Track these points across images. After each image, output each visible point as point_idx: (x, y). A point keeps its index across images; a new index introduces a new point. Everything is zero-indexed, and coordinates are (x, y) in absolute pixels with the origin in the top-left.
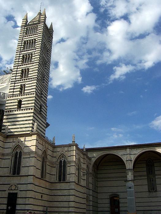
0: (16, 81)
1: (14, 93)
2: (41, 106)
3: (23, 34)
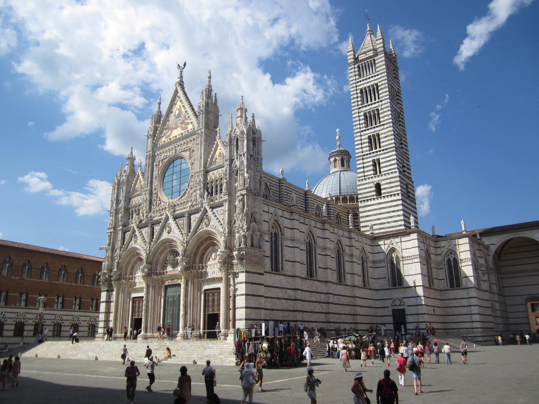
0: (364, 155)
1: (366, 174)
2: (407, 186)
3: (354, 78)
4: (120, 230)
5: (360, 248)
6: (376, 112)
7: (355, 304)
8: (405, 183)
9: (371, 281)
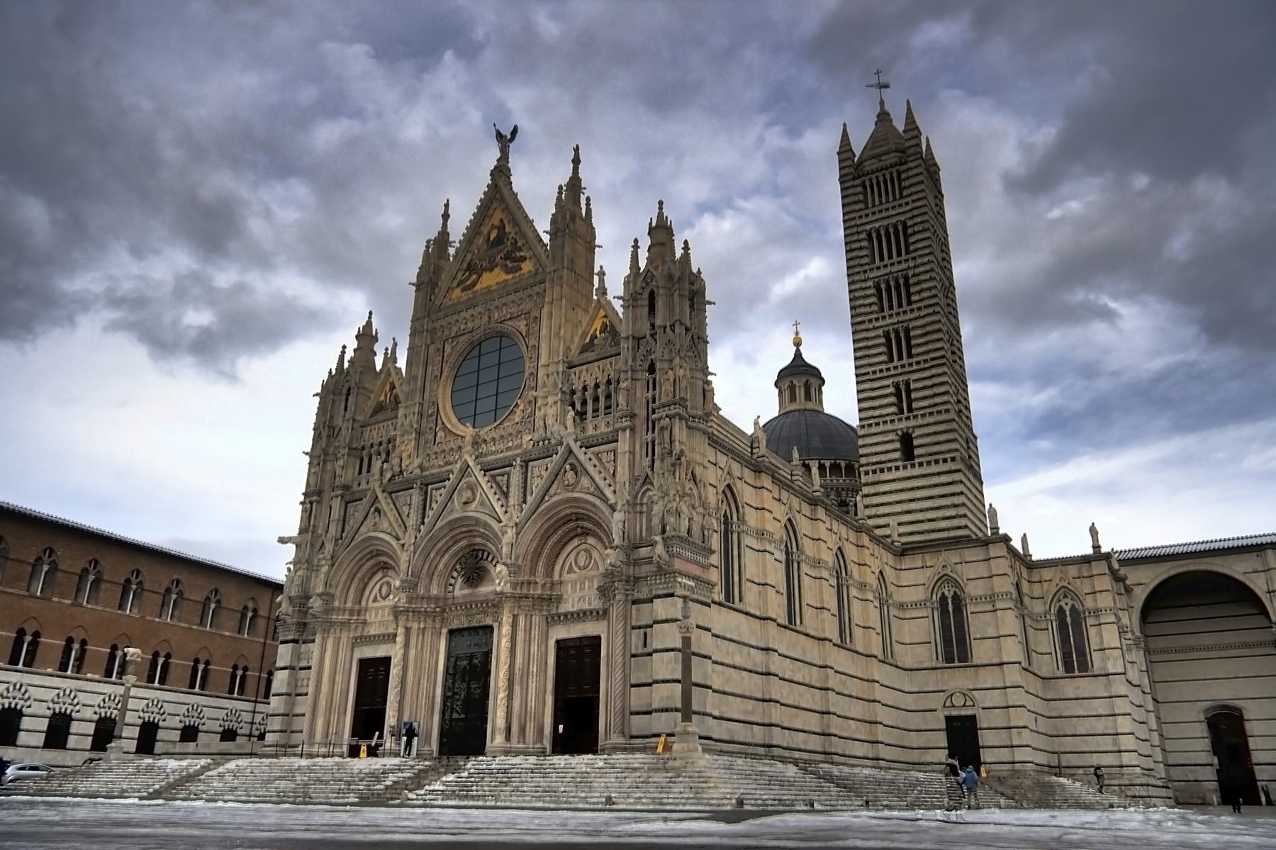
0: (874, 372)
1: (877, 413)
2: (967, 443)
4: (337, 496)
5: (877, 572)
6: (901, 281)
7: (871, 698)
8: (964, 436)
9: (896, 646)
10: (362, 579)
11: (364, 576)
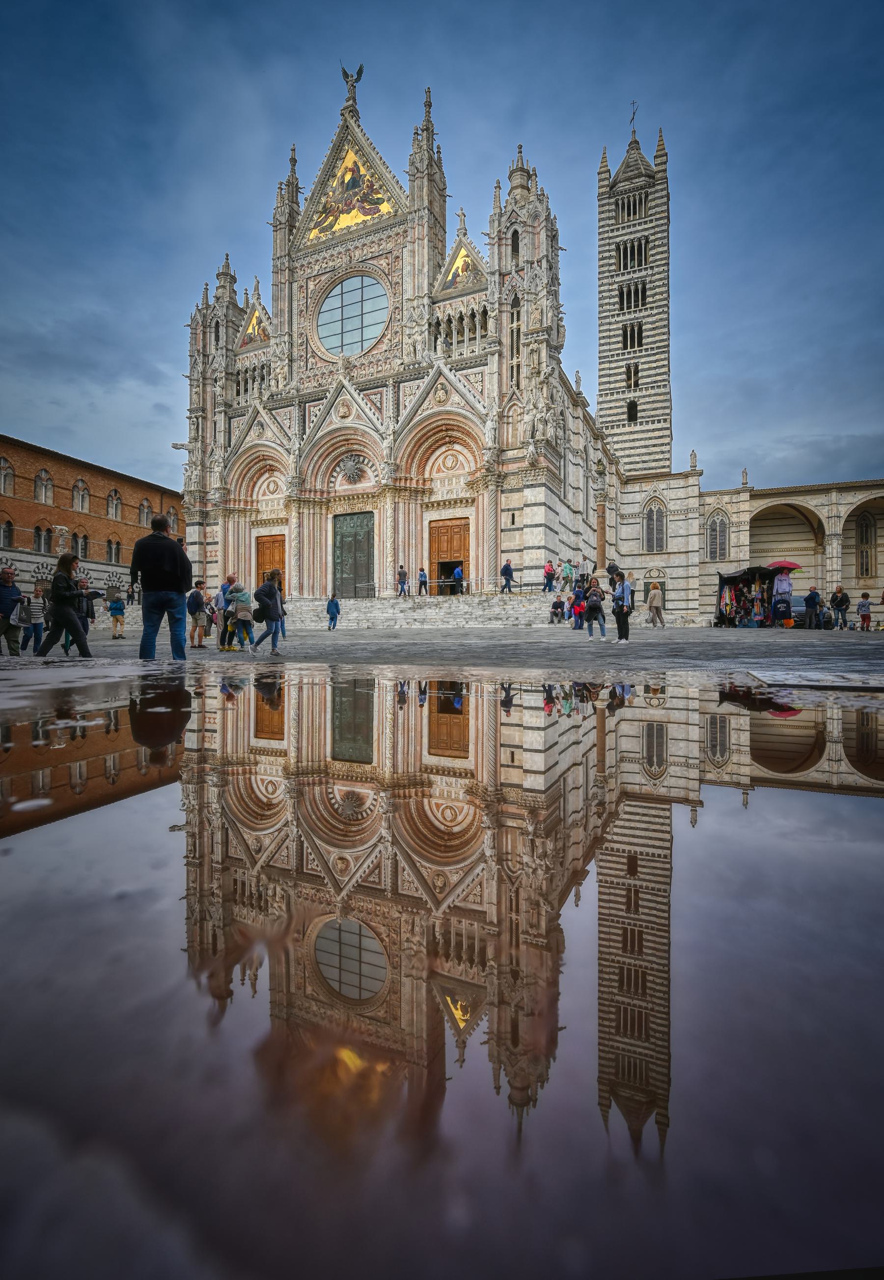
4: (220, 412)
10: (252, 478)
11: (253, 476)
